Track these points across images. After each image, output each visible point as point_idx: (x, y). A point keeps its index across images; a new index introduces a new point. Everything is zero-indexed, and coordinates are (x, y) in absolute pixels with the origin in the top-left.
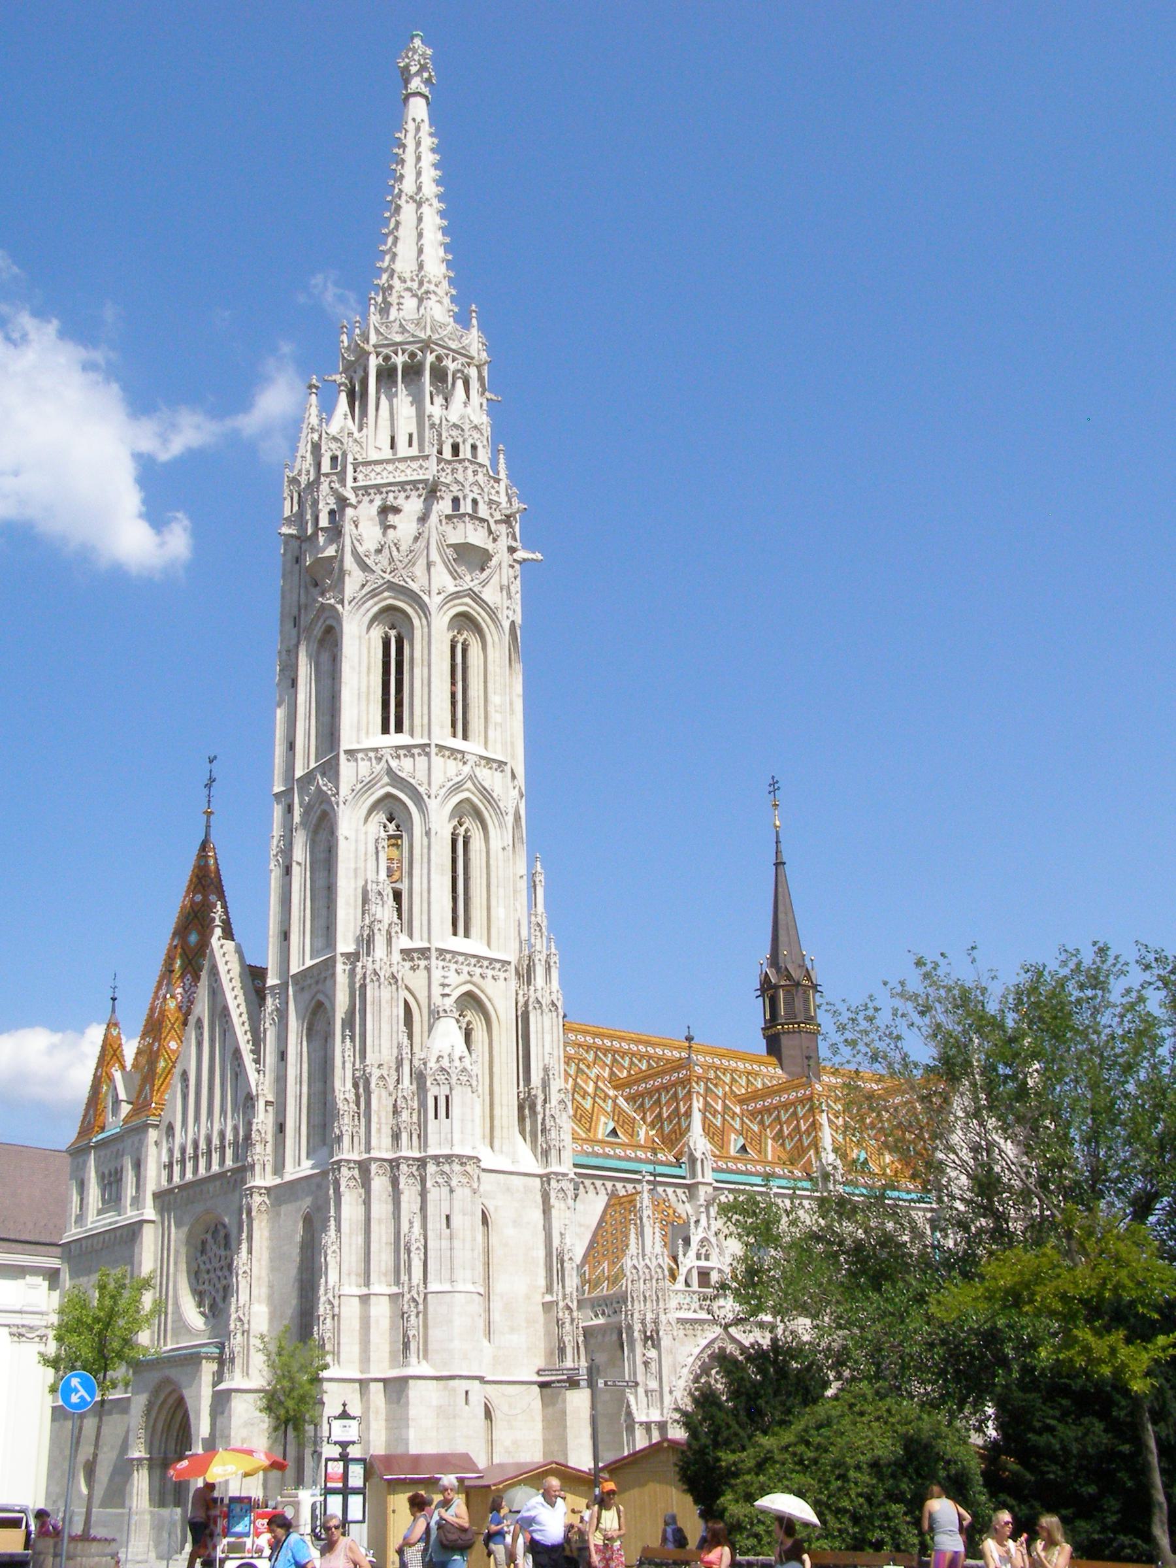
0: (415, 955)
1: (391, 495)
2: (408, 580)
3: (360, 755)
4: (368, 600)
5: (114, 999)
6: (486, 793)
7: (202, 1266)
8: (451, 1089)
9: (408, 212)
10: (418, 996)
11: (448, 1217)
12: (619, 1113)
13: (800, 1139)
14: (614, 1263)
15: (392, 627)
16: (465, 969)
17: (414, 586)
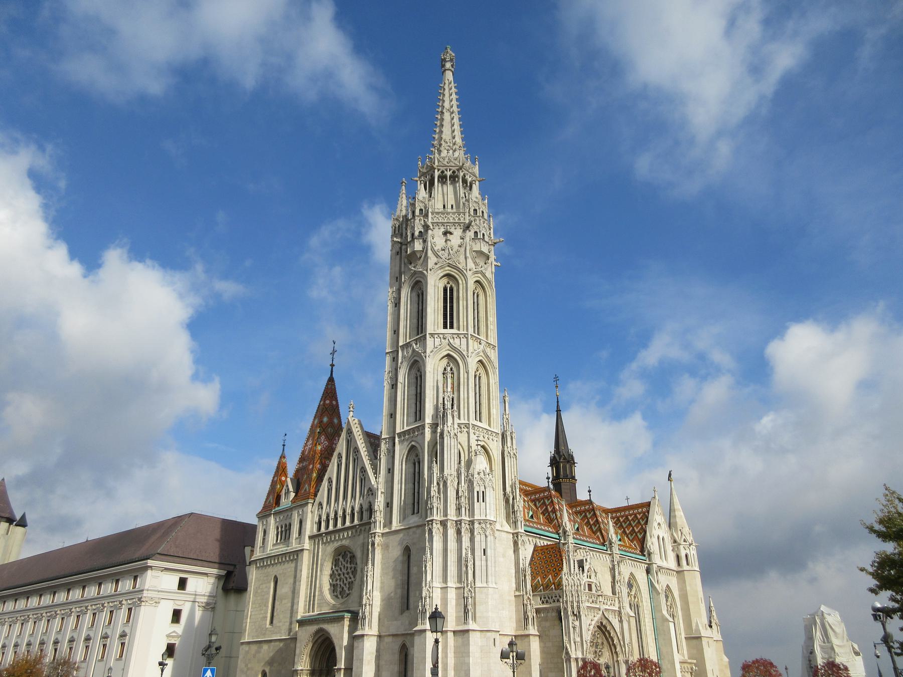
2: (457, 263)
3: (436, 336)
4: (438, 270)
5: (284, 445)
7: (335, 572)
8: (485, 488)
14: (544, 578)
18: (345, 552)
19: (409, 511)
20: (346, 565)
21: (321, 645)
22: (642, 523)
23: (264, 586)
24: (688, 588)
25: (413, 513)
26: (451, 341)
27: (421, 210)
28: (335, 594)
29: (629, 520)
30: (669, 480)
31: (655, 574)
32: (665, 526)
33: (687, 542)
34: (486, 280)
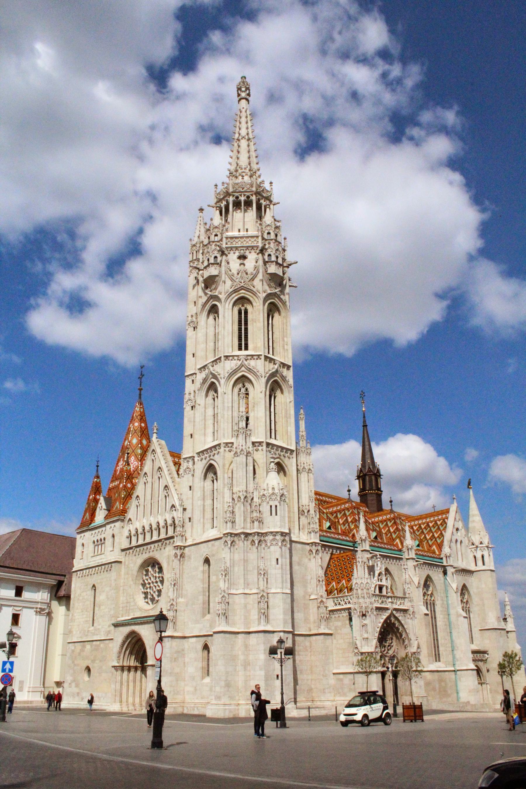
1: (242, 251)
3: (231, 358)
5: (98, 466)
6: (284, 378)
11: (277, 559)
13: (391, 535)
14: (338, 583)
15: (243, 306)
17: (254, 290)
18: (154, 564)
19: (208, 525)
20: (154, 575)
21: (135, 645)
22: (441, 528)
23: (84, 594)
25: (213, 527)
26: (246, 363)
28: (146, 600)
29: (429, 527)
30: (468, 487)
32: (462, 532)
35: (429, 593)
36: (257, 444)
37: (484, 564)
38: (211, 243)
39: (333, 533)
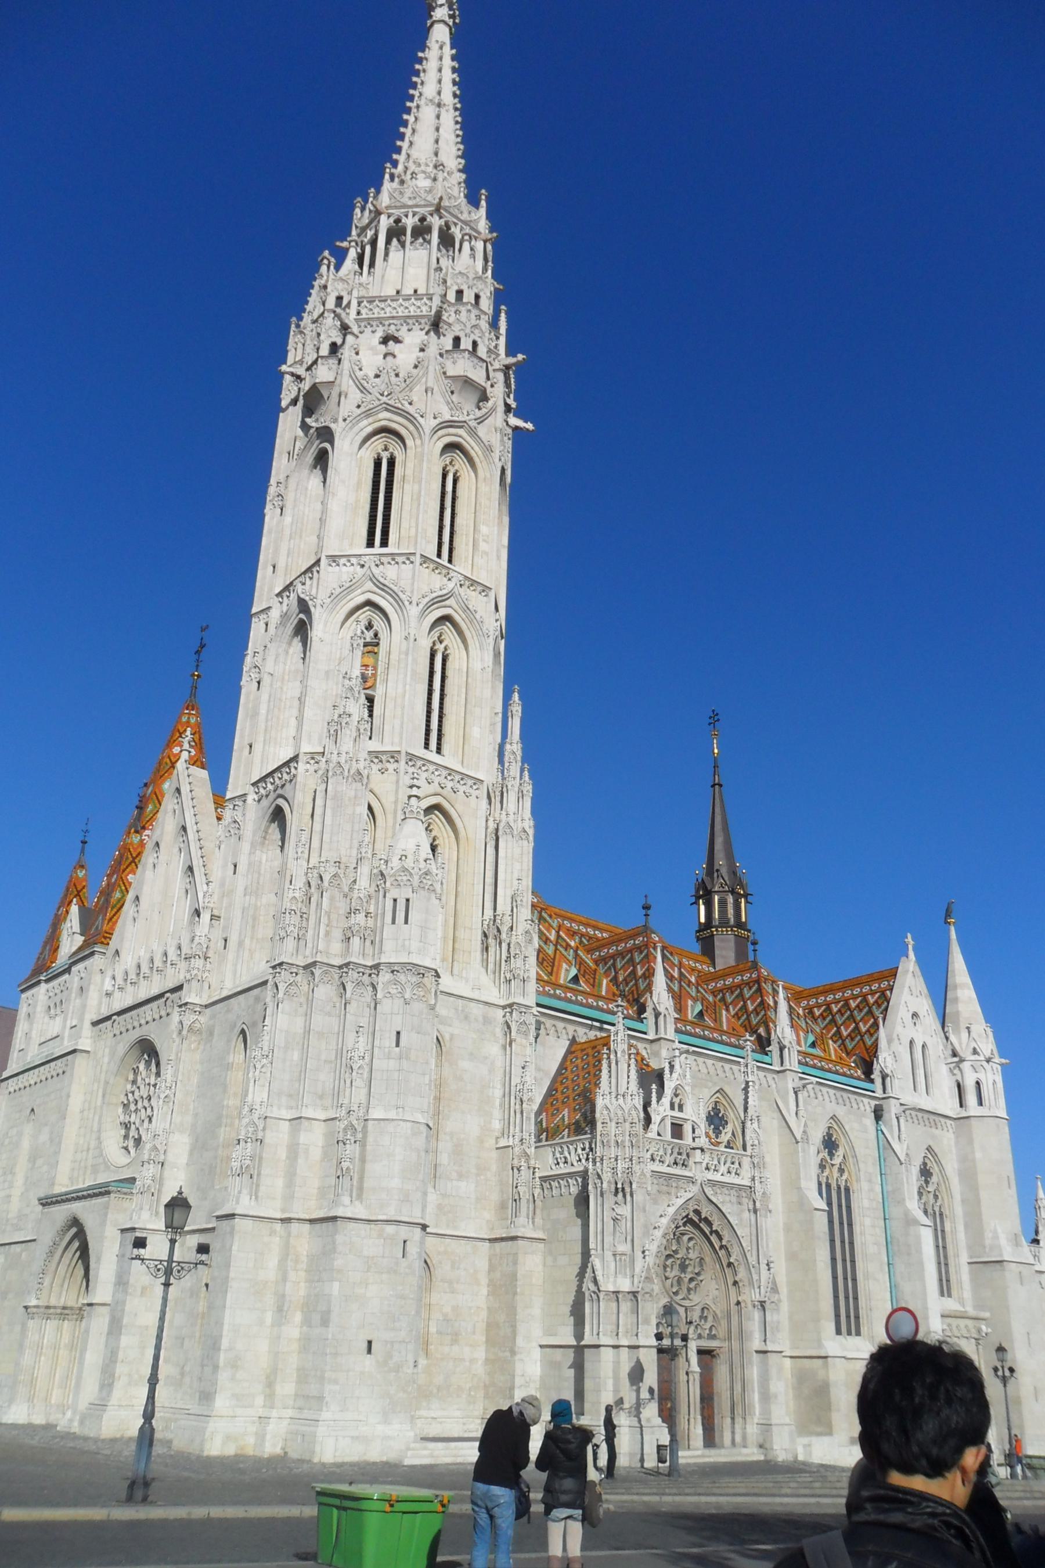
0: (384, 758)
1: (393, 327)
3: (343, 561)
4: (361, 420)
9: (427, 113)
10: (383, 801)
11: (398, 1033)
12: (580, 964)
13: (748, 1018)
15: (386, 449)
16: (437, 780)
17: (411, 409)
24: (978, 1155)
26: (375, 570)
27: (339, 299)
30: (946, 922)
31: (895, 1121)
32: (930, 1019)
33: (978, 1054)
34: (478, 445)
35: (837, 1160)
36: (384, 758)
37: (980, 1103)
38: (326, 314)
39: (583, 992)
